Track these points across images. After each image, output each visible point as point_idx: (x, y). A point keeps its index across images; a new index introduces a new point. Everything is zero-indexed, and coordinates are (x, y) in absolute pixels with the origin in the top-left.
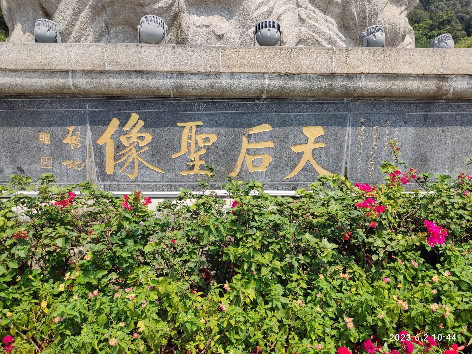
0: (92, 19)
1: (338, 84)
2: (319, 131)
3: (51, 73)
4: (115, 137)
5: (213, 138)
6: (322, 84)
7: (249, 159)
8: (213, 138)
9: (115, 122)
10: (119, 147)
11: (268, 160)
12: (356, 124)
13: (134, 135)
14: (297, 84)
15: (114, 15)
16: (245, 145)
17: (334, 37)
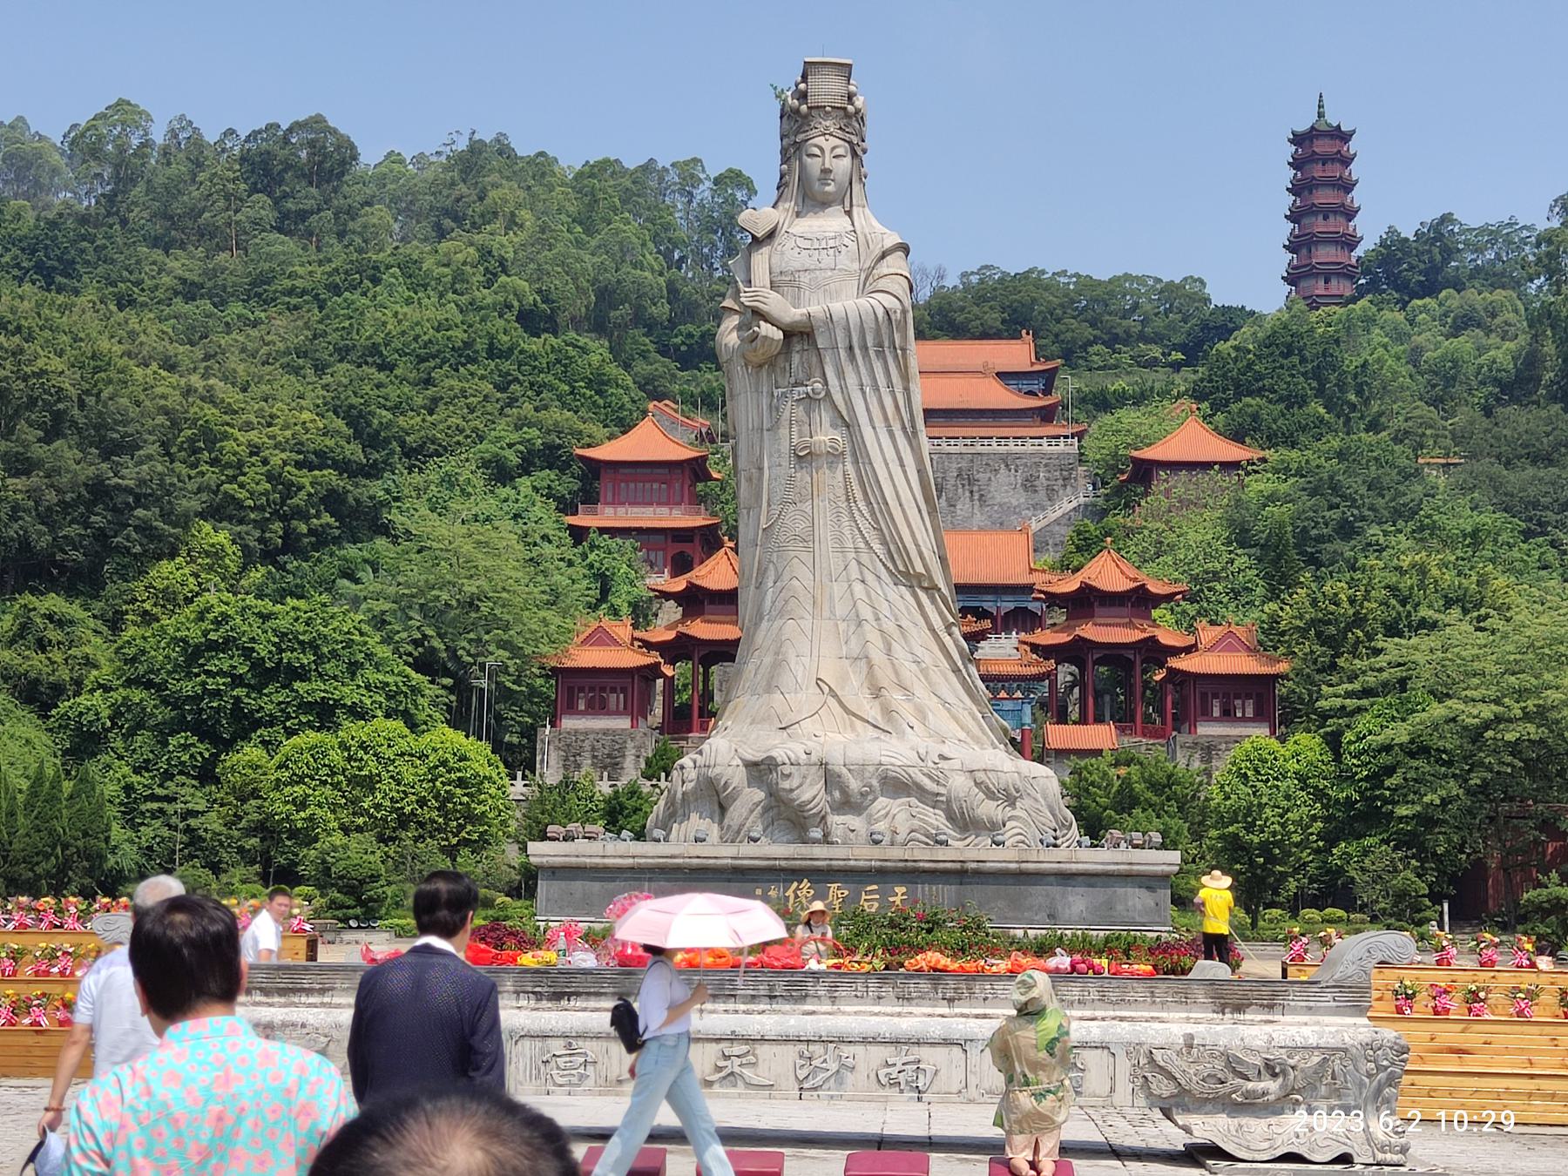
0: (762, 815)
1: (909, 864)
2: (904, 889)
3: (769, 859)
4: (794, 892)
5: (846, 893)
6: (901, 864)
7: (866, 904)
8: (846, 893)
9: (795, 884)
10: (797, 897)
11: (876, 905)
12: (923, 883)
13: (805, 891)
14: (889, 864)
15: (779, 814)
16: (864, 897)
17: (942, 826)
